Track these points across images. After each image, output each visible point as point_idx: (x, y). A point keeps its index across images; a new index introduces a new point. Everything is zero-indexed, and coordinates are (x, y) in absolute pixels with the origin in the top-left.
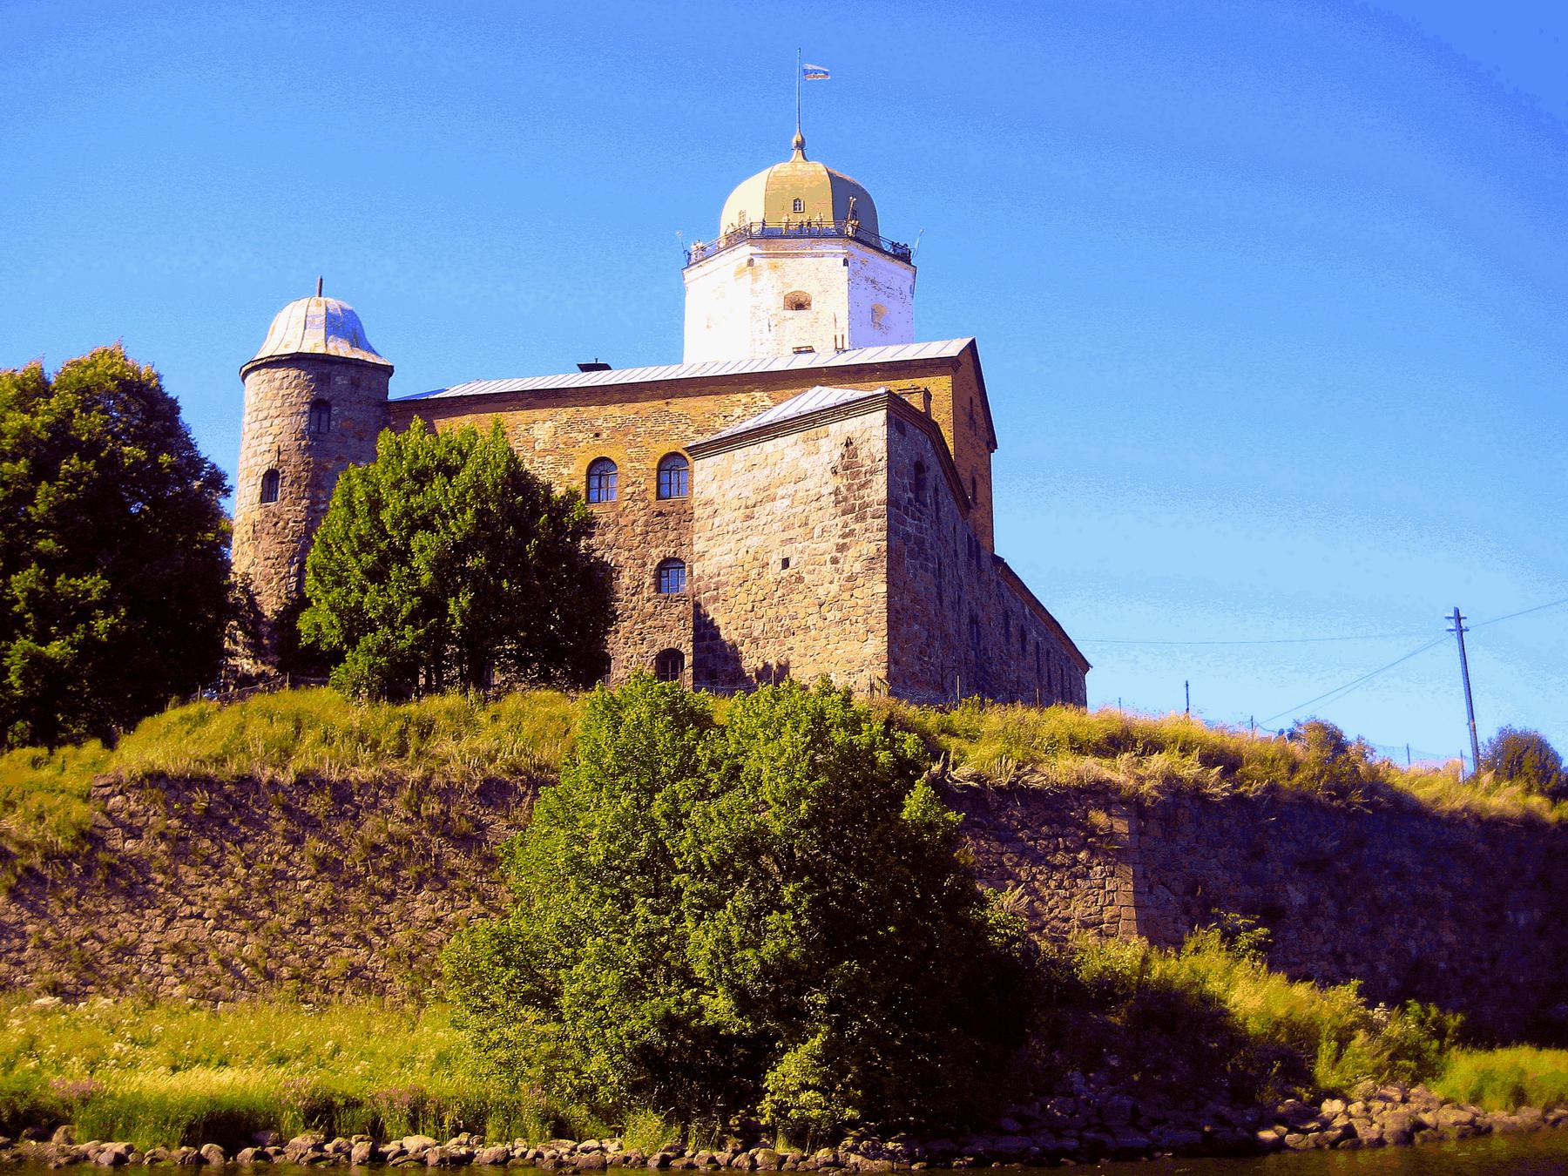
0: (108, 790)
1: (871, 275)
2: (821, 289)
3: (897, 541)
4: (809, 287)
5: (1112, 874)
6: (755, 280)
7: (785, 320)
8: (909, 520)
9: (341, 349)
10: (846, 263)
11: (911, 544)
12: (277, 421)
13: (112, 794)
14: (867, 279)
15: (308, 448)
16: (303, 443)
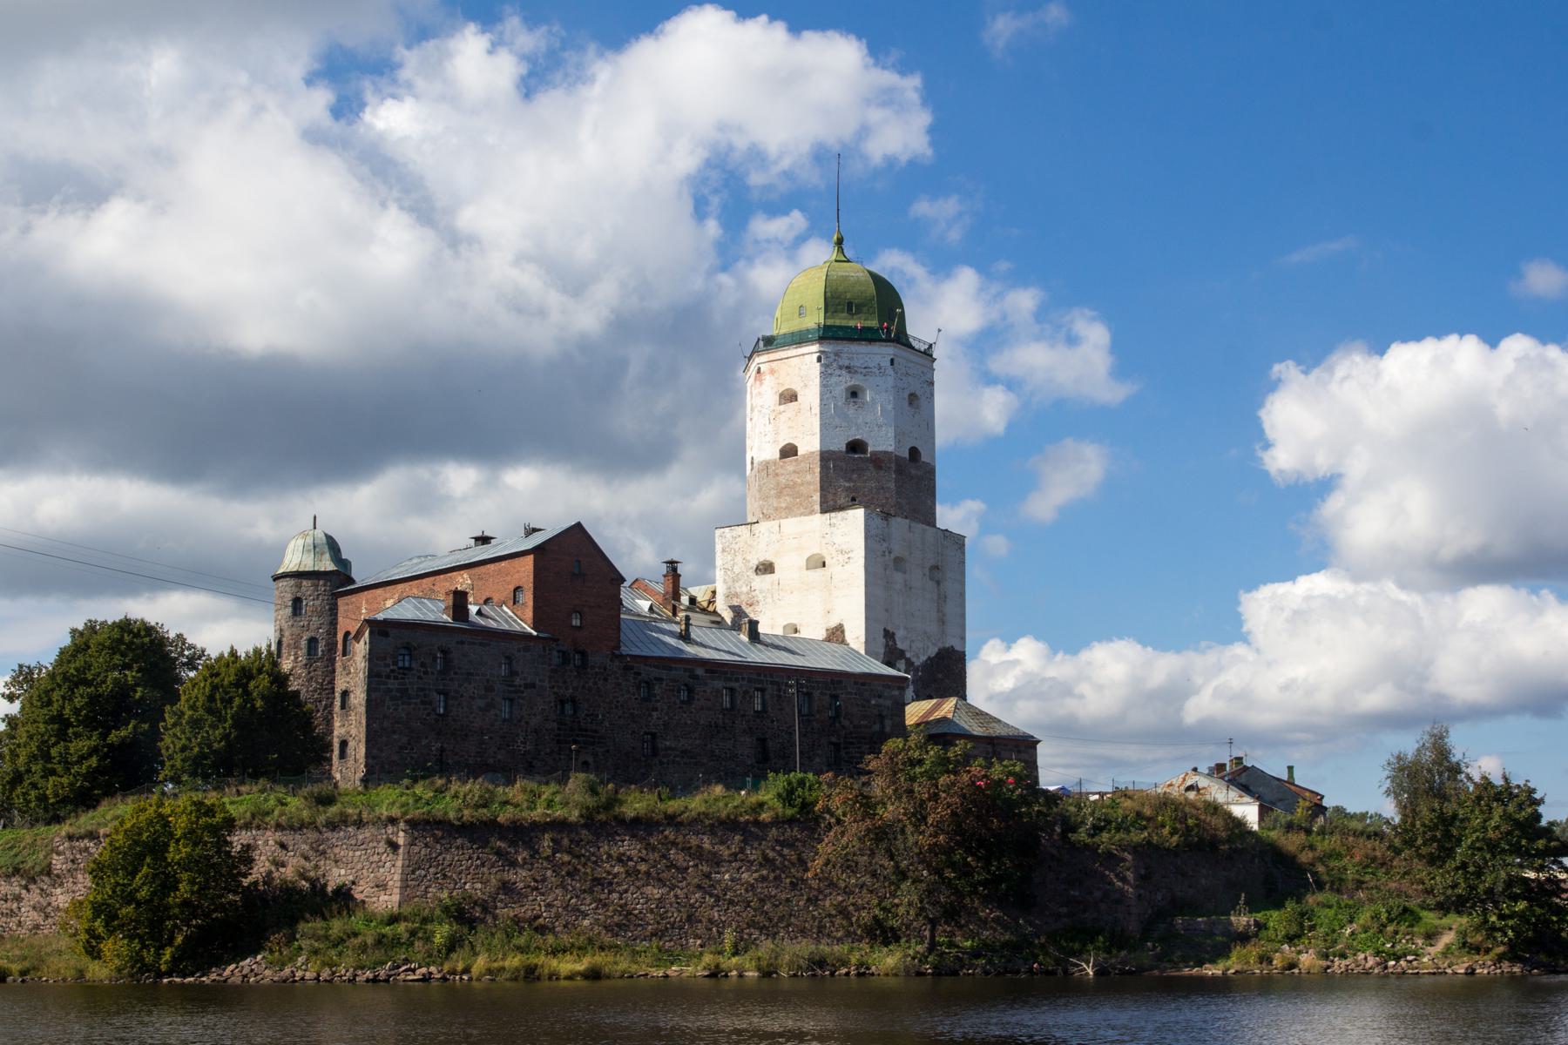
0: (58, 844)
1: (846, 364)
2: (802, 384)
3: (374, 696)
4: (797, 387)
5: (394, 866)
6: (761, 384)
7: (780, 413)
8: (392, 681)
9: (309, 564)
10: (819, 360)
11: (394, 693)
12: (281, 612)
13: (60, 845)
14: (840, 368)
15: (292, 626)
16: (290, 624)
